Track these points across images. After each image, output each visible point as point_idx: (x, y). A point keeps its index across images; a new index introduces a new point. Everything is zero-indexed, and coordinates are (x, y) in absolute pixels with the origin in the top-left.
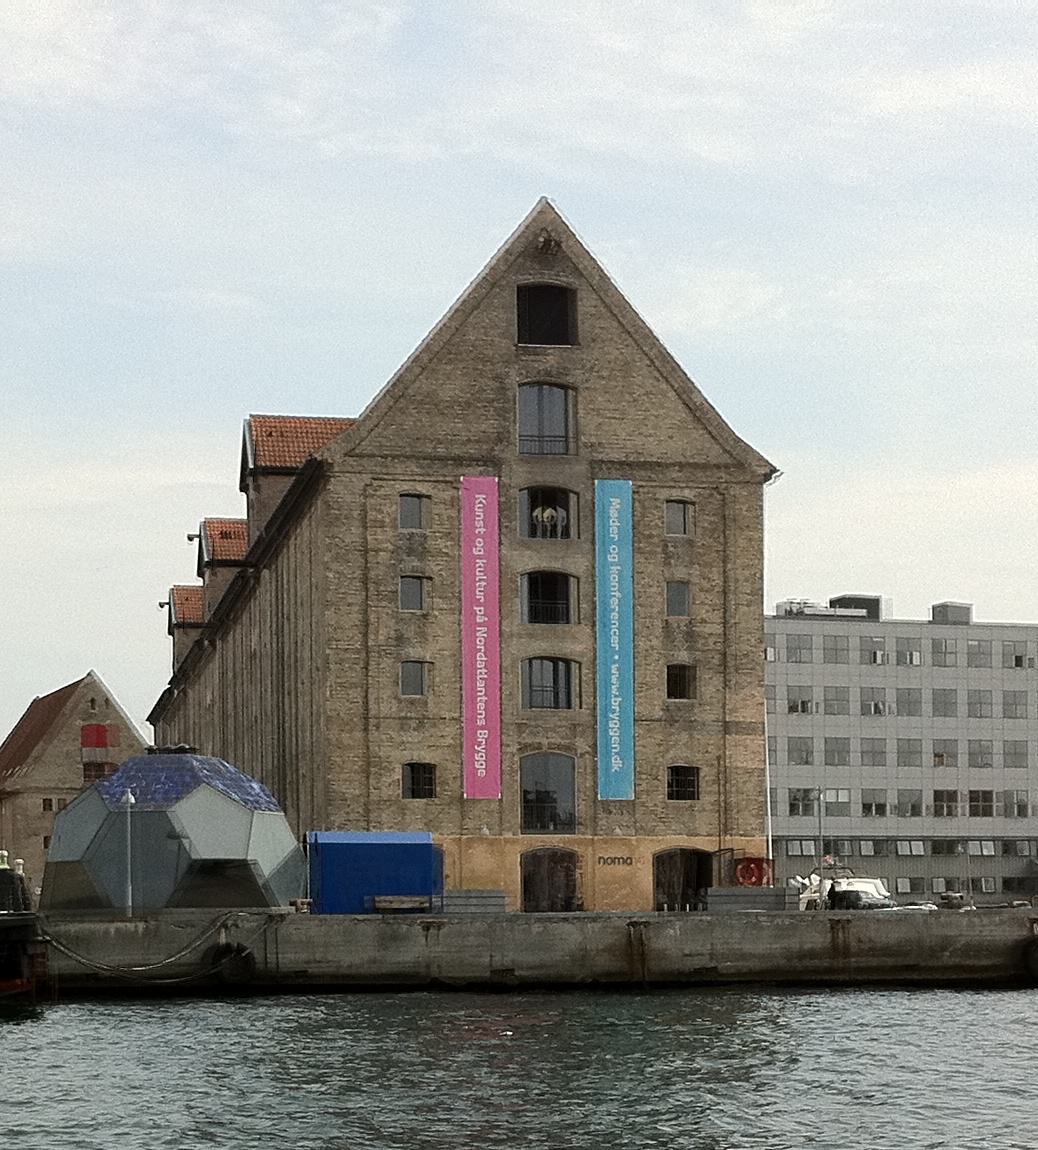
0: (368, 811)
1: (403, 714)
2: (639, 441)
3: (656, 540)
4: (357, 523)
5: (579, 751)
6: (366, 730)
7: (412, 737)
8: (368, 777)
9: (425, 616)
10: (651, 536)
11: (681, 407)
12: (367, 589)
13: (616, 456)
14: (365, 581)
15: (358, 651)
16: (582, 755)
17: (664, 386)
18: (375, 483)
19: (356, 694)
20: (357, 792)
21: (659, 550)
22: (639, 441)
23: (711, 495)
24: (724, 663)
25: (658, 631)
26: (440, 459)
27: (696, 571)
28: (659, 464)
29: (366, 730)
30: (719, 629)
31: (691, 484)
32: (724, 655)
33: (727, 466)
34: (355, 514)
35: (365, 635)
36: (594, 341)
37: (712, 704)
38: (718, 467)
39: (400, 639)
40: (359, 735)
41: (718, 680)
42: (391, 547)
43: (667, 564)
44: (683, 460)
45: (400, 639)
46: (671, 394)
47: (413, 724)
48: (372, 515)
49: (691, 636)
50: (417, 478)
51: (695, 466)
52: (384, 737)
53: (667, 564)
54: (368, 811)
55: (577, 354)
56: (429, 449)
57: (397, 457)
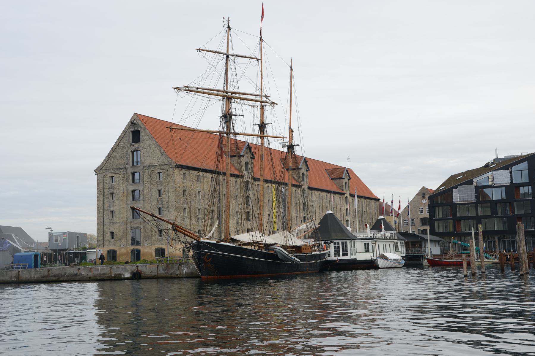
0: (103, 242)
1: (110, 222)
2: (152, 161)
3: (155, 181)
4: (102, 183)
5: (141, 228)
6: (104, 226)
7: (111, 227)
8: (104, 236)
9: (114, 201)
10: (154, 181)
11: (160, 153)
12: (104, 197)
13: (148, 164)
14: (104, 195)
15: (102, 210)
16: (142, 228)
17: (157, 149)
18: (106, 175)
19: (102, 218)
20: (102, 239)
21: (156, 184)
22: (152, 161)
23: (165, 171)
24: (168, 207)
25: (156, 201)
26: (116, 169)
27: (163, 187)
28: (155, 165)
29: (104, 226)
30: (167, 199)
31: (161, 169)
32: (168, 205)
33: (168, 165)
34: (102, 182)
35: (104, 206)
36: (144, 141)
37: (166, 216)
38: (166, 165)
39: (110, 207)
40: (102, 227)
41: (167, 211)
42: (108, 188)
43: (157, 186)
44: (160, 164)
45: (110, 207)
46: (158, 150)
47: (112, 224)
48: (105, 181)
49: (162, 202)
50: (112, 173)
51: (162, 165)
52: (107, 227)
53: (157, 186)
54: (103, 242)
55: (141, 145)
56: (115, 167)
57: (108, 169)
